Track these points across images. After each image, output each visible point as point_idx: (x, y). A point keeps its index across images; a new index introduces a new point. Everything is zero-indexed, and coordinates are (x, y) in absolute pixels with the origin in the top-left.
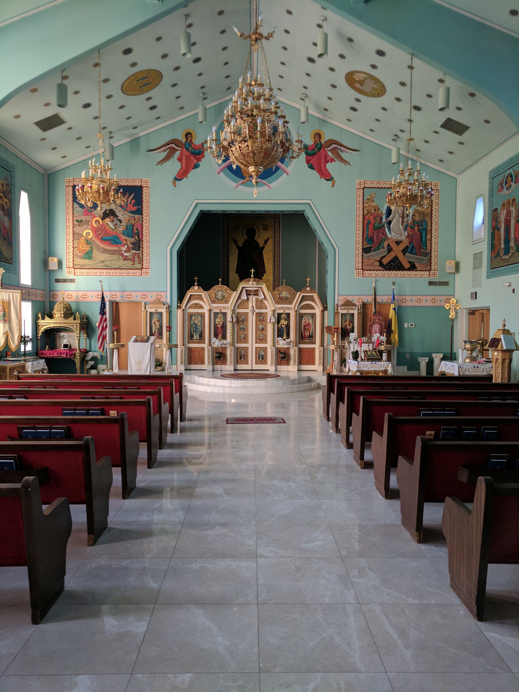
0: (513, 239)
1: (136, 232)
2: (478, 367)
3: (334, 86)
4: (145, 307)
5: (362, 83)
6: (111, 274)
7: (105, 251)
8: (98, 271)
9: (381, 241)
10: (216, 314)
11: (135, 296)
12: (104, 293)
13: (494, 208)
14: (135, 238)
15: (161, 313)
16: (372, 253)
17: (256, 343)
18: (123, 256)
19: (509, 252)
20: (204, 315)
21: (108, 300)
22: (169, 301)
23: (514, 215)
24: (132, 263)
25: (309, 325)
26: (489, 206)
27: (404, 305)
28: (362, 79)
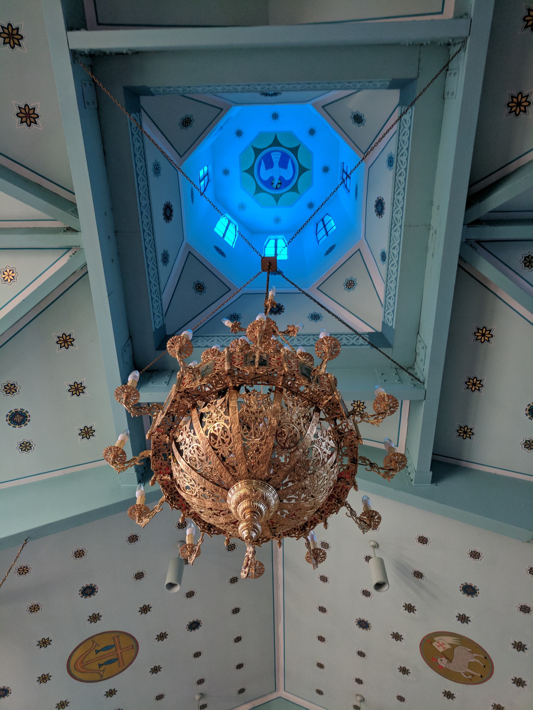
3: (404, 671)
5: (448, 655)
28: (448, 647)
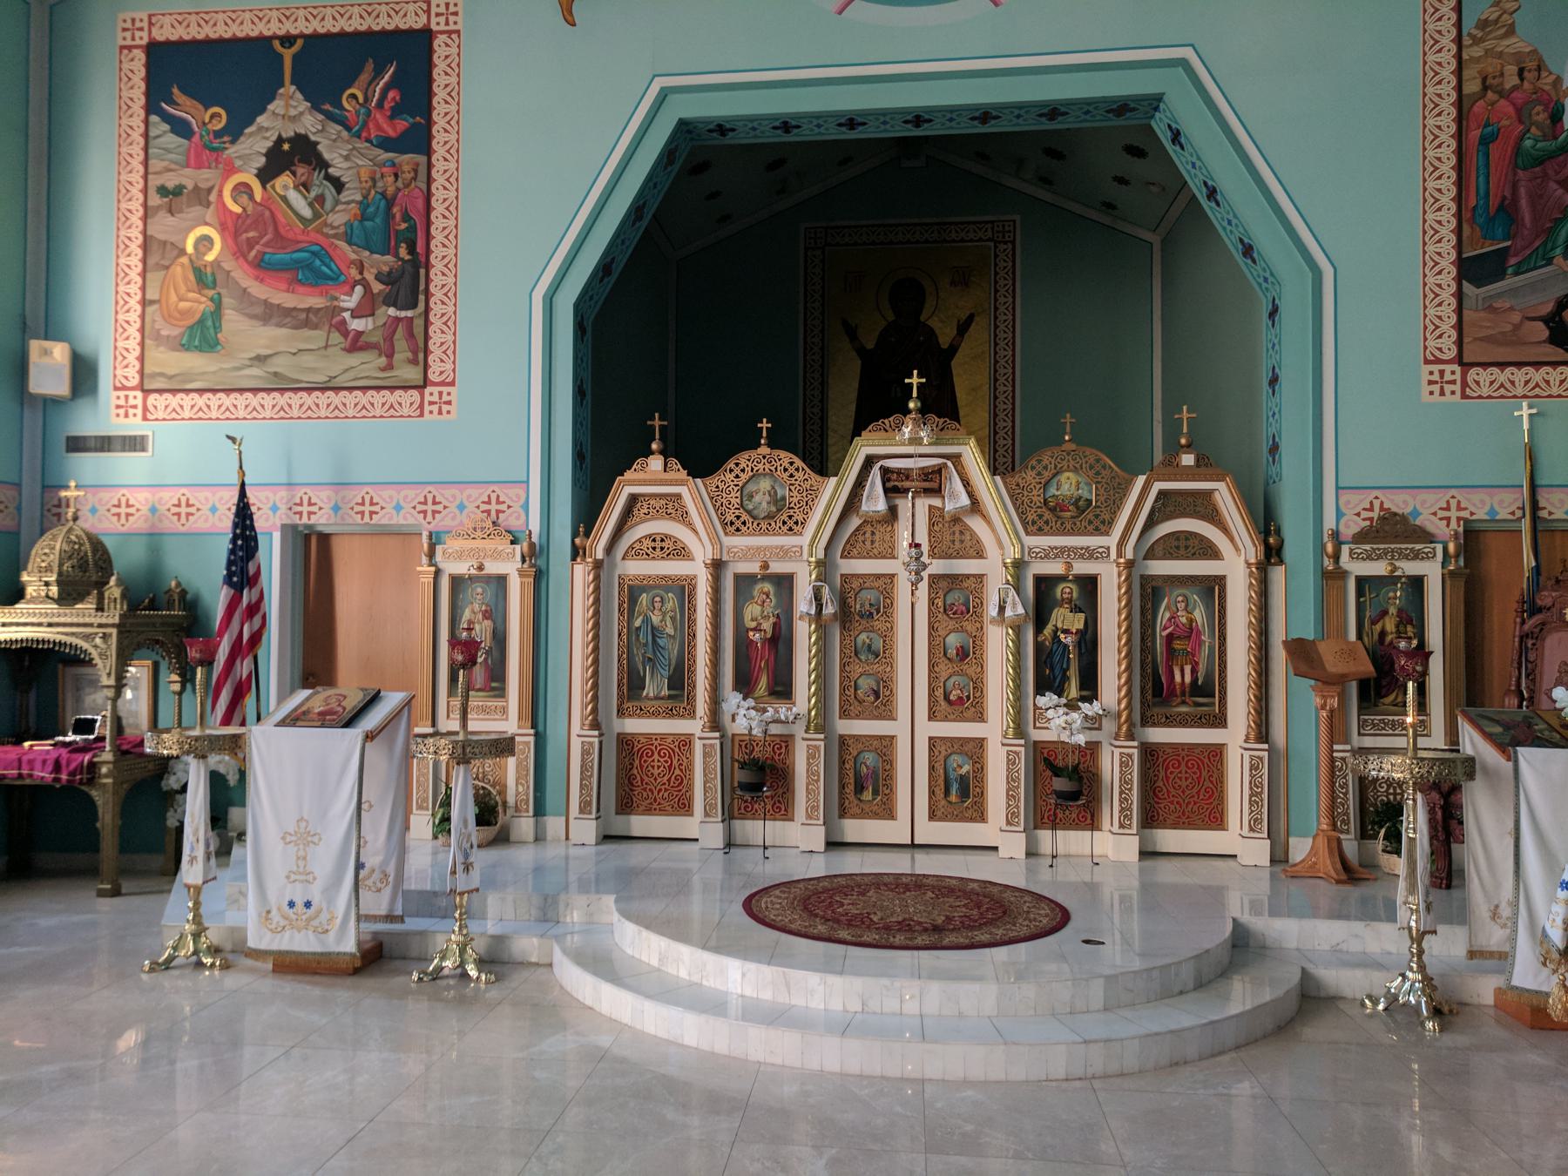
1: (404, 226)
6: (295, 413)
7: (270, 314)
8: (240, 400)
12: (249, 493)
14: (396, 255)
16: (1509, 282)
17: (932, 716)
18: (345, 333)
20: (693, 588)
21: (278, 524)
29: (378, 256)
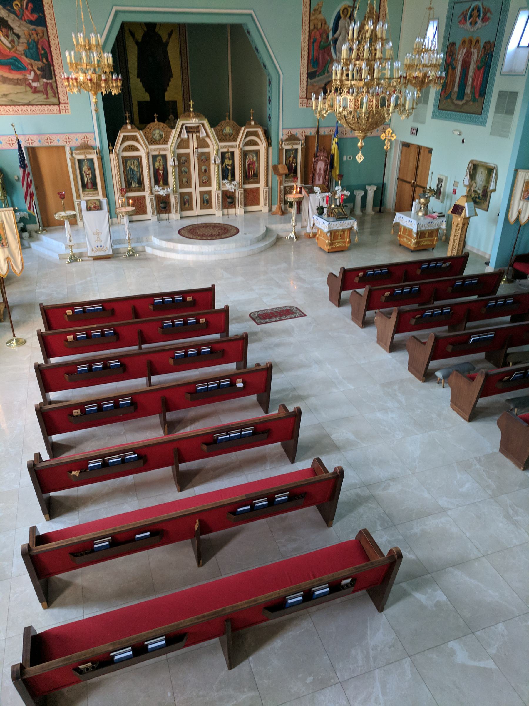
0: (470, 86)
1: (43, 52)
2: (432, 222)
4: (72, 154)
9: (326, 64)
10: (154, 157)
11: (56, 141)
13: (451, 41)
14: (43, 62)
15: (92, 160)
19: (463, 99)
22: (98, 144)
23: (475, 58)
24: (45, 96)
25: (253, 163)
26: (445, 37)
27: (345, 137)
29: (36, 62)
